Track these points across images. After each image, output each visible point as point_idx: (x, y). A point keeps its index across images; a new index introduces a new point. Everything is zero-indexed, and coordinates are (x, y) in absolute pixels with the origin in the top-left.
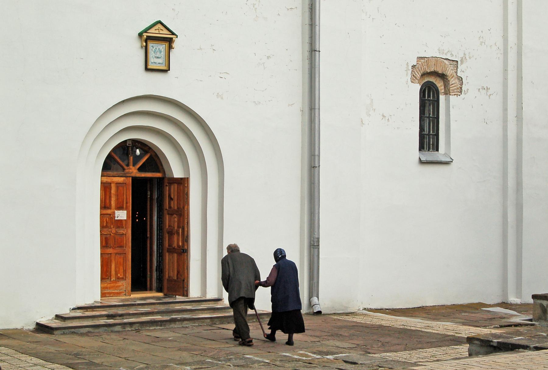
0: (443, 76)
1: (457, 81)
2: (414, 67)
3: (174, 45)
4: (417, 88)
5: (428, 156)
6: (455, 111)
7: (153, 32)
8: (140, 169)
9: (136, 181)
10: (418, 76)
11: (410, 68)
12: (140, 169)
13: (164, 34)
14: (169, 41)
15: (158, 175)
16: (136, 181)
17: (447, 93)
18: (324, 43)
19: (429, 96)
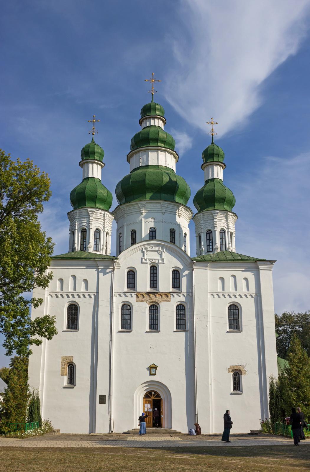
0: (240, 370)
1: (244, 371)
2: (229, 368)
3: (158, 368)
4: (231, 374)
5: (236, 392)
6: (244, 380)
7: (152, 366)
8: (155, 397)
9: (153, 400)
10: (231, 371)
11: (228, 369)
12: (155, 397)
13: (154, 366)
14: (156, 368)
15: (159, 399)
16: (153, 400)
17: (242, 375)
18: (109, 372)
19: (237, 376)
